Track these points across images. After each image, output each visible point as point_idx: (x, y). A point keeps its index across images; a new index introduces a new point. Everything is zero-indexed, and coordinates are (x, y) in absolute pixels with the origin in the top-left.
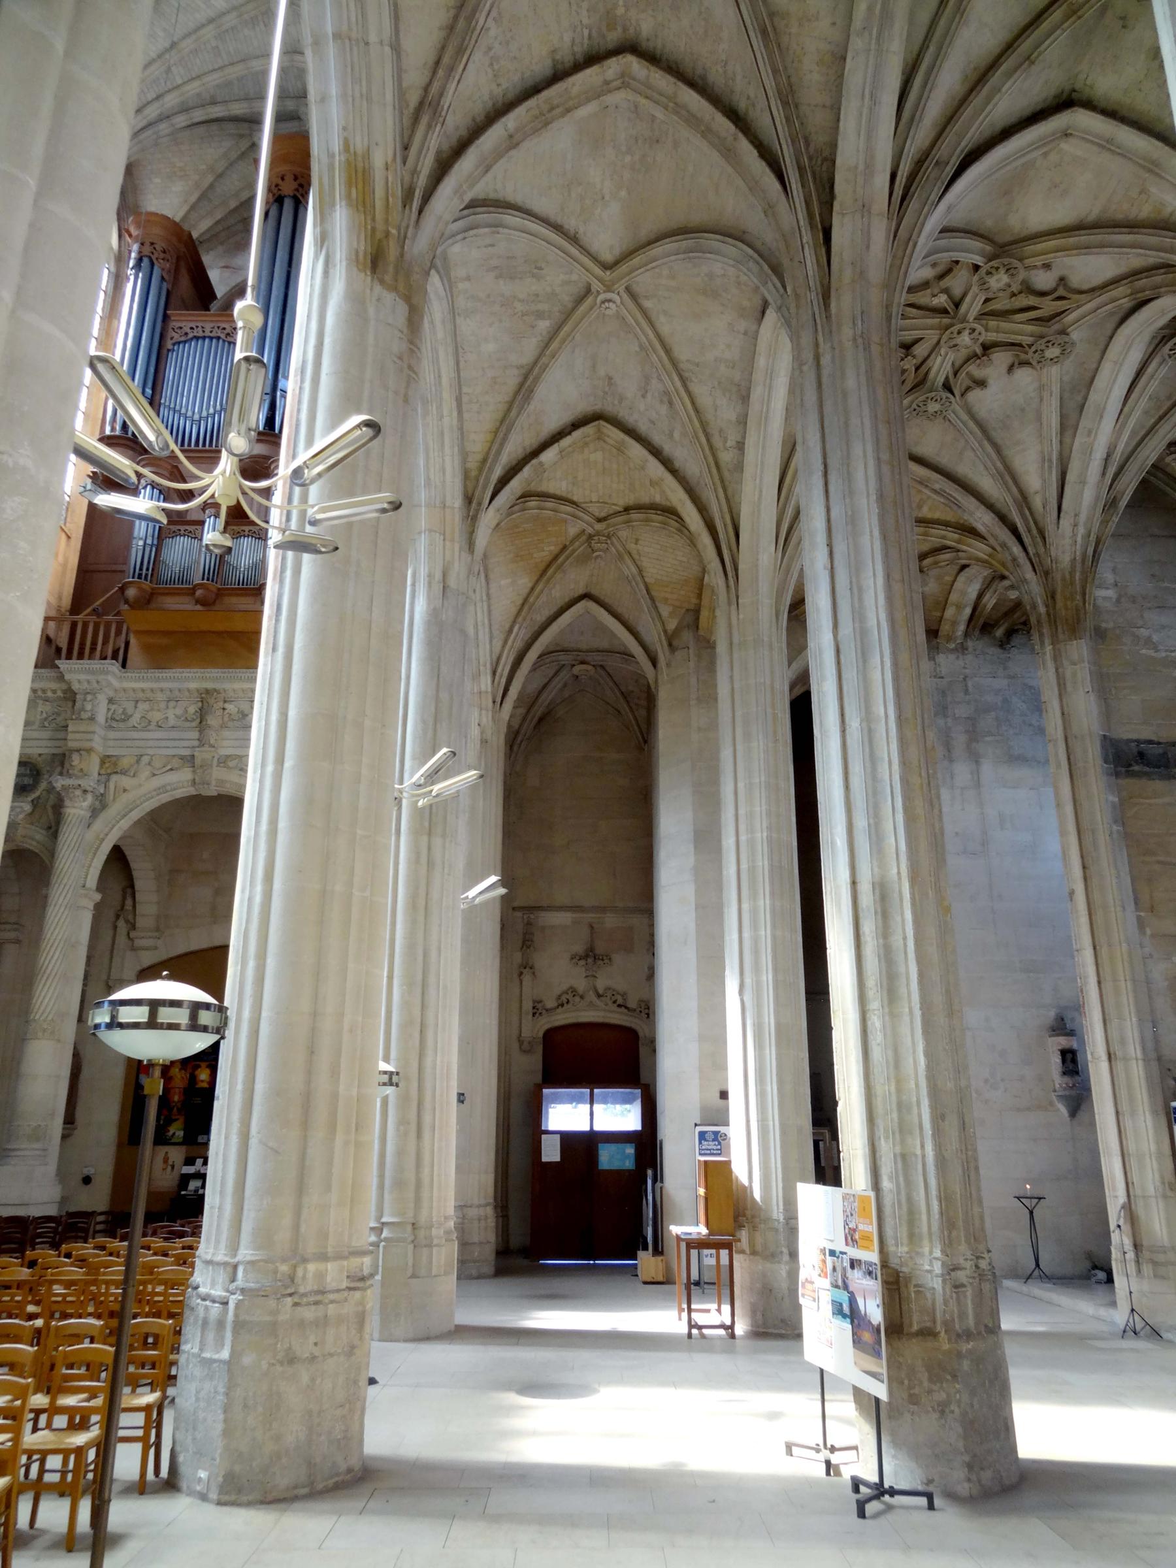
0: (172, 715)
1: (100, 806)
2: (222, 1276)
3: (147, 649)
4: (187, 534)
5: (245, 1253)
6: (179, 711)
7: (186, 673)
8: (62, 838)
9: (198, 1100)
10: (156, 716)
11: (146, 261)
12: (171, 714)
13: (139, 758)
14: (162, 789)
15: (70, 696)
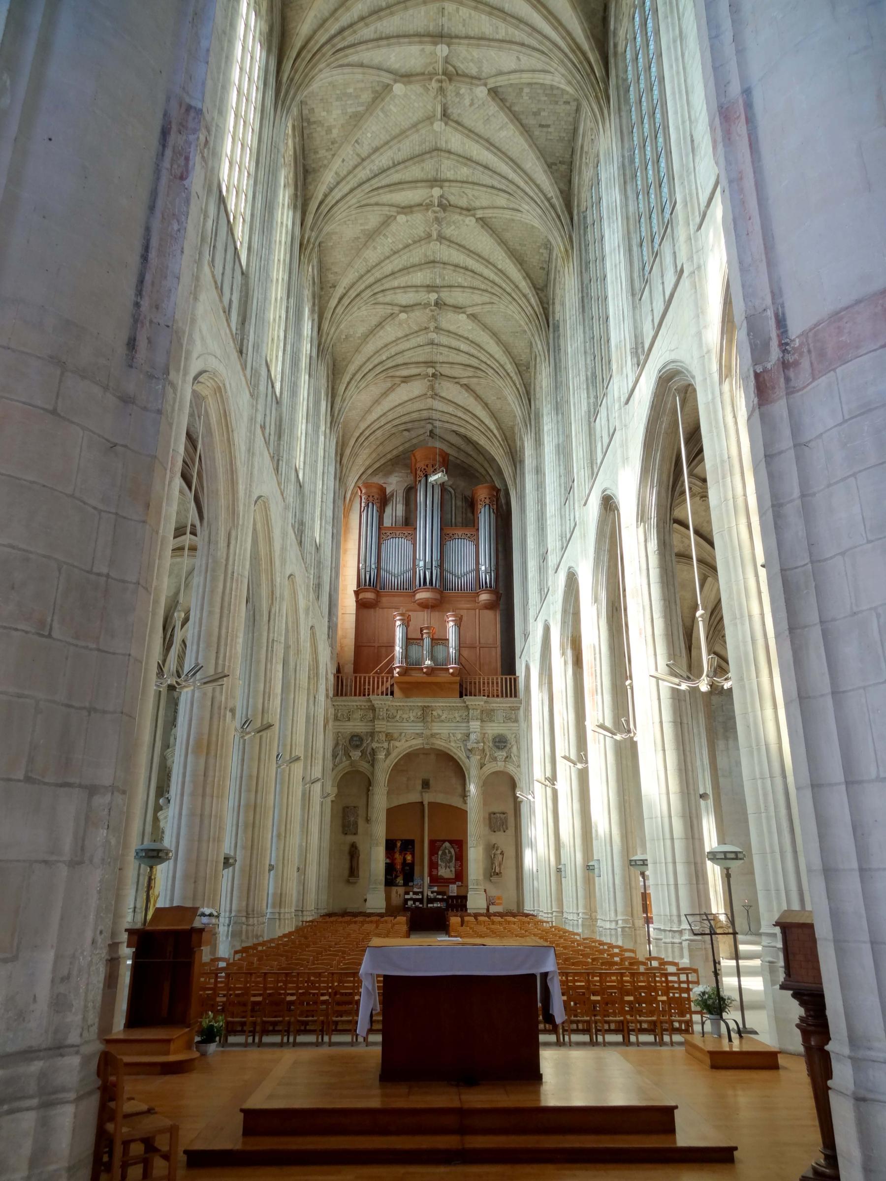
0: (412, 715)
1: (388, 754)
2: (575, 915)
3: (401, 689)
4: (417, 644)
5: (581, 910)
6: (414, 714)
7: (418, 699)
8: (376, 767)
9: (407, 868)
10: (405, 716)
11: (370, 505)
12: (411, 715)
13: (401, 733)
14: (410, 747)
15: (373, 709)
